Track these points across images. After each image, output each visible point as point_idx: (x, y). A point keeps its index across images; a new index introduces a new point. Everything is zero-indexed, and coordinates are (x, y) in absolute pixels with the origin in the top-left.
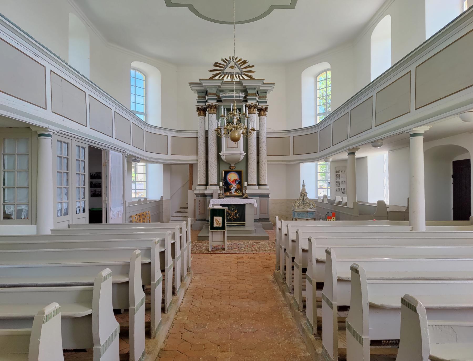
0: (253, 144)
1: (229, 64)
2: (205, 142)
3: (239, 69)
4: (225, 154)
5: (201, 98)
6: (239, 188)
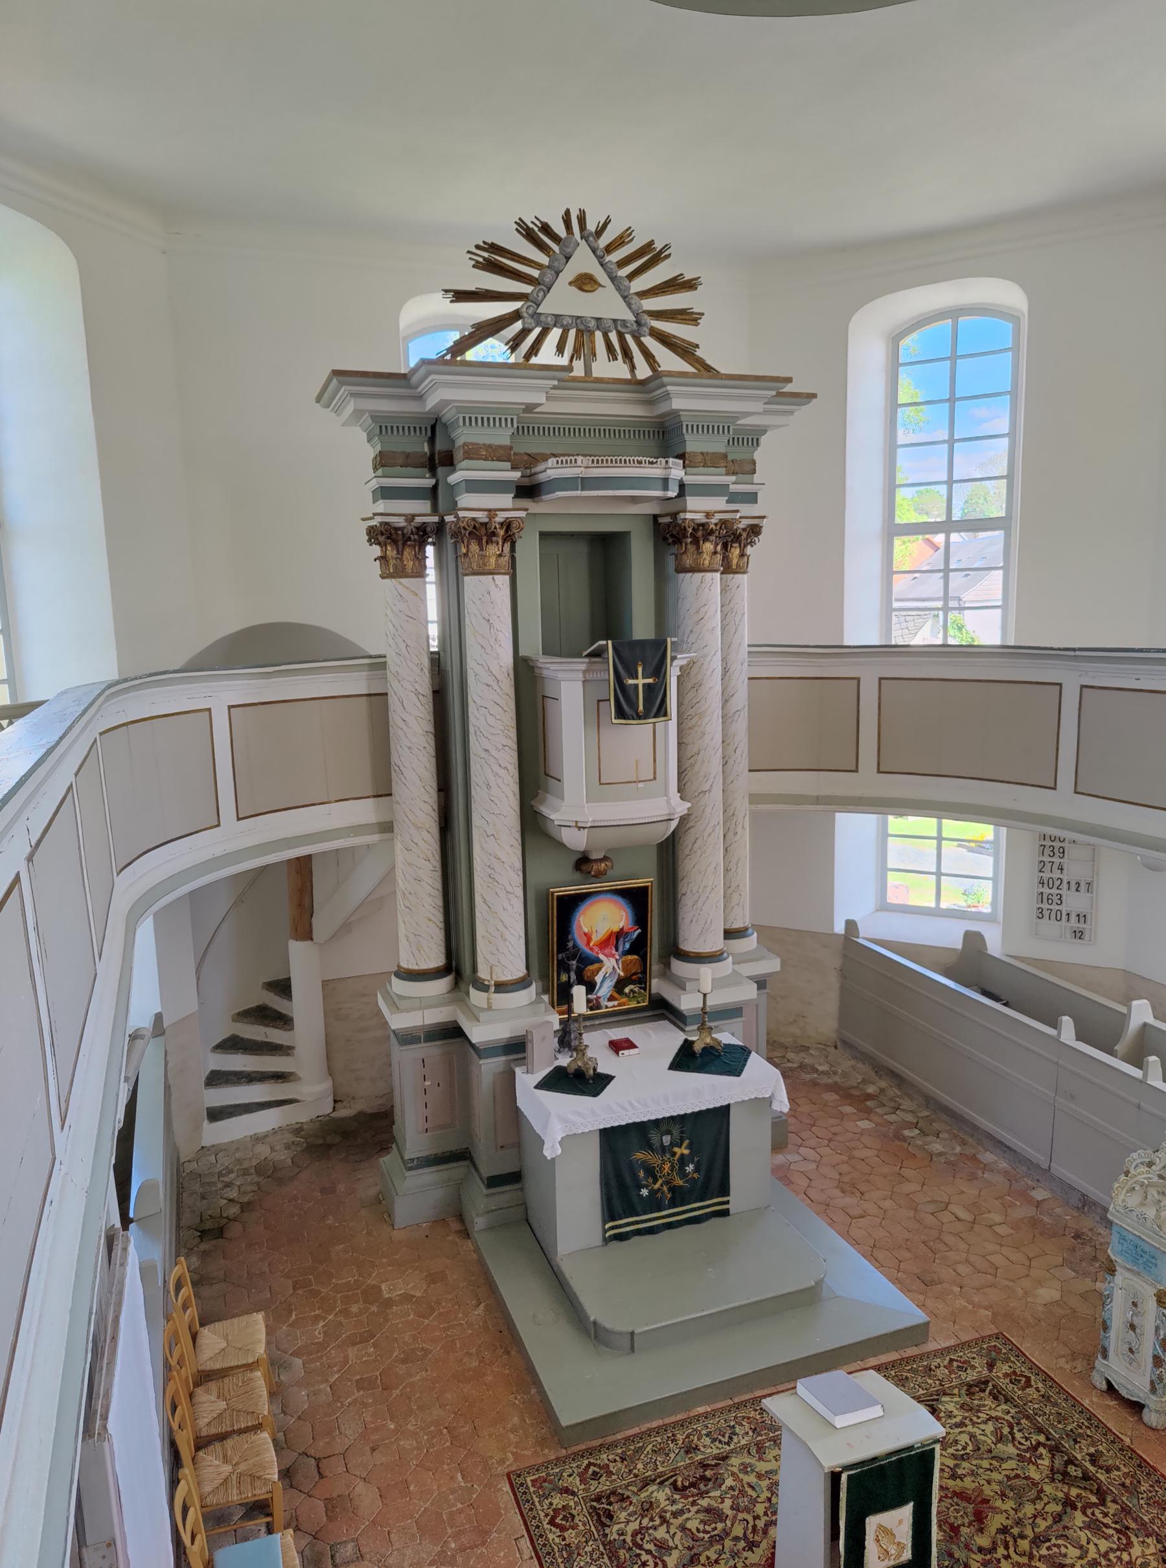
1: (568, 258)
2: (430, 728)
3: (624, 298)
5: (401, 466)
6: (633, 971)
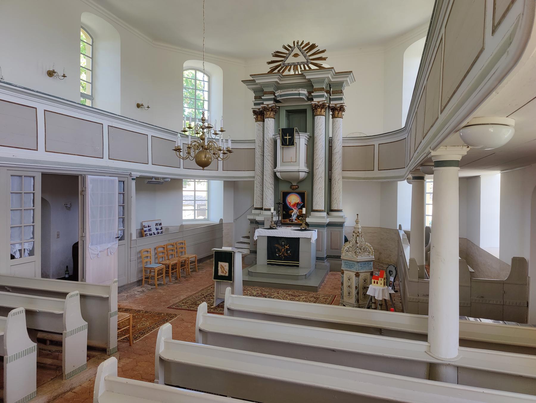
0: (319, 156)
1: (292, 51)
3: (305, 57)
4: (279, 171)
